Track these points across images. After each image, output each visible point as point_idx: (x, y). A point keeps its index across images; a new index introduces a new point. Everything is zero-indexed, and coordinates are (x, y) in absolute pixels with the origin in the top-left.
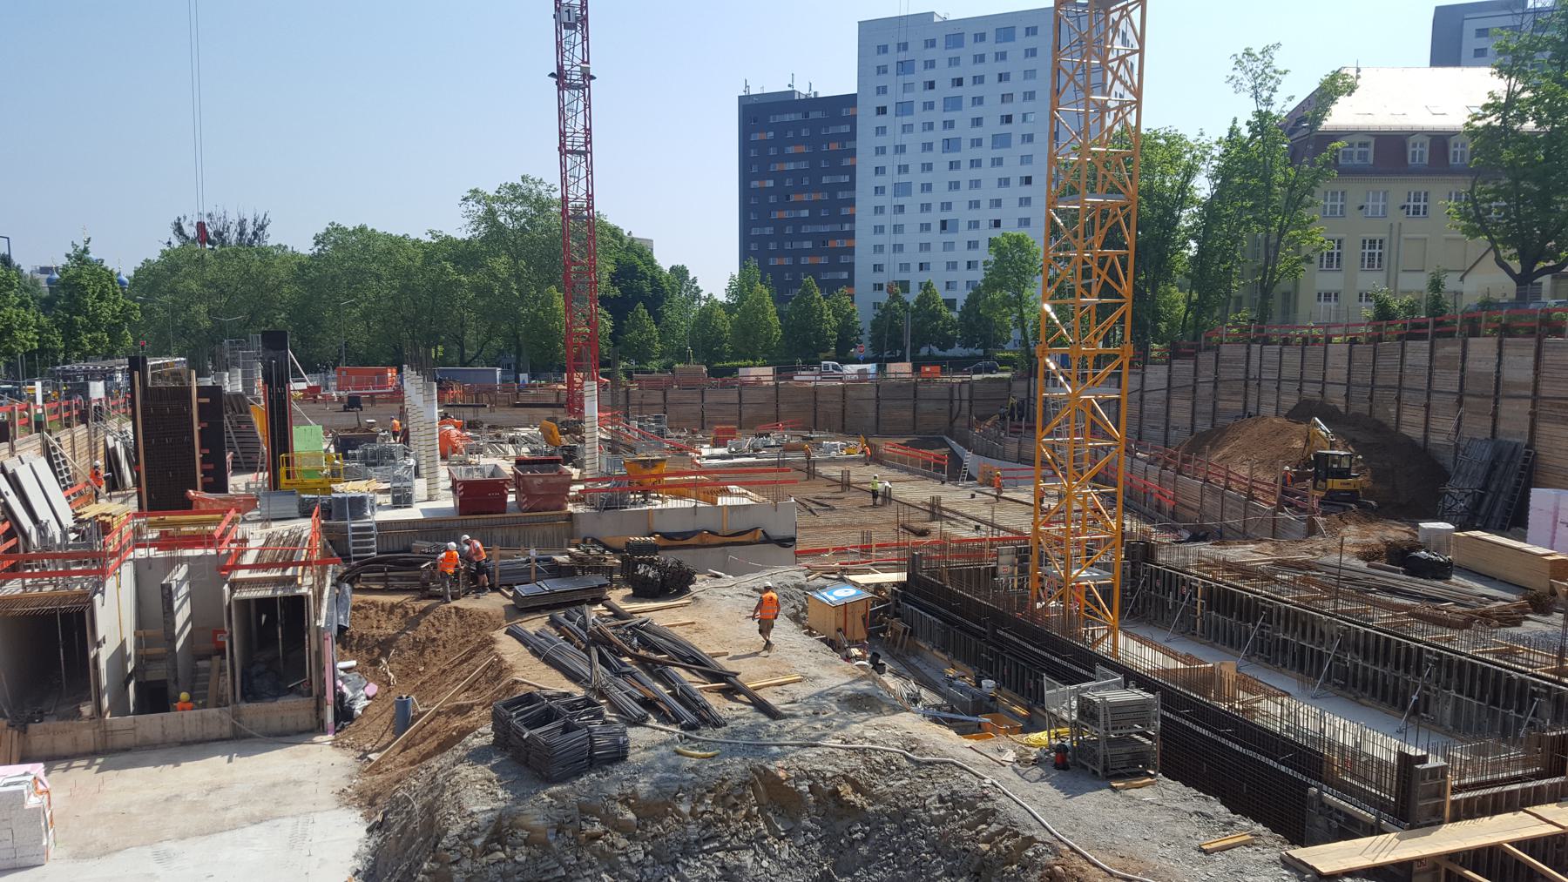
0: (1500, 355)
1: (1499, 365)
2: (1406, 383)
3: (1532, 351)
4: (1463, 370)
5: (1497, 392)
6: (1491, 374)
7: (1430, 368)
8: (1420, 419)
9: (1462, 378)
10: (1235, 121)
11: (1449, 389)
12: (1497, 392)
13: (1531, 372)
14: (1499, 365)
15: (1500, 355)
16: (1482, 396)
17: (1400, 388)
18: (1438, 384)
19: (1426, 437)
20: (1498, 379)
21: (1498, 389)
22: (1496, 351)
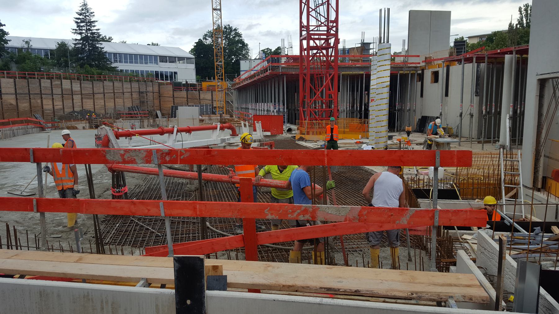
0: (72, 84)
1: (72, 87)
2: (43, 92)
3: (79, 84)
4: (62, 88)
5: (72, 93)
6: (70, 89)
7: (52, 87)
8: (51, 102)
9: (62, 90)
10: (94, 12)
11: (58, 93)
12: (72, 93)
13: (80, 88)
14: (72, 87)
15: (72, 84)
16: (68, 95)
17: (41, 94)
18: (54, 92)
19: (54, 108)
20: (72, 90)
21: (72, 93)
22: (71, 83)
